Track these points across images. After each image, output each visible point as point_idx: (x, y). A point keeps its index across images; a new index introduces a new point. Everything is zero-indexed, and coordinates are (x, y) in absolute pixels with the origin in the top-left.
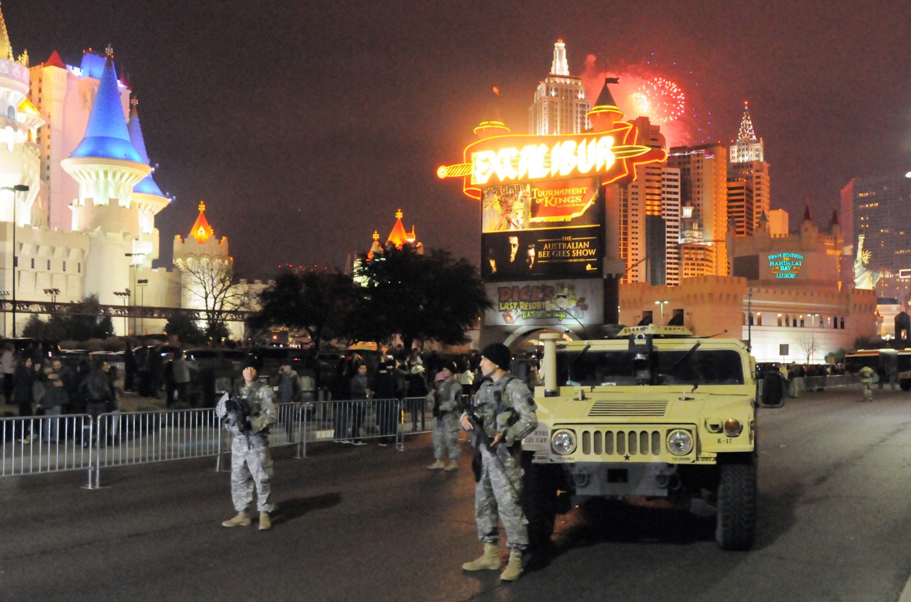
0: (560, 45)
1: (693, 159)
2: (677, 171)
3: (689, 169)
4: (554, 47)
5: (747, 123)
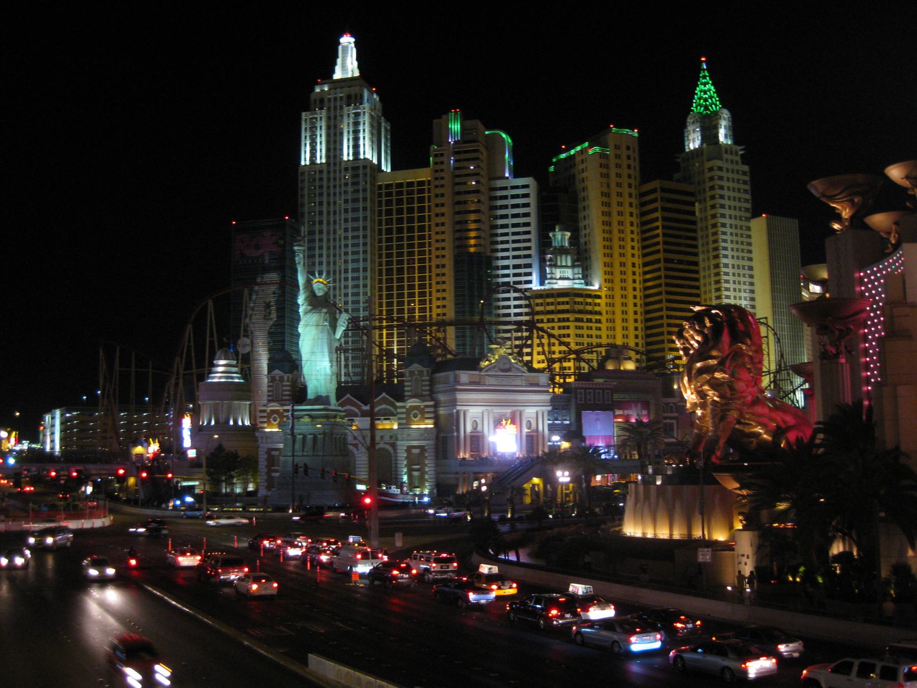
0: (347, 41)
1: (578, 159)
3: (574, 175)
4: (339, 43)
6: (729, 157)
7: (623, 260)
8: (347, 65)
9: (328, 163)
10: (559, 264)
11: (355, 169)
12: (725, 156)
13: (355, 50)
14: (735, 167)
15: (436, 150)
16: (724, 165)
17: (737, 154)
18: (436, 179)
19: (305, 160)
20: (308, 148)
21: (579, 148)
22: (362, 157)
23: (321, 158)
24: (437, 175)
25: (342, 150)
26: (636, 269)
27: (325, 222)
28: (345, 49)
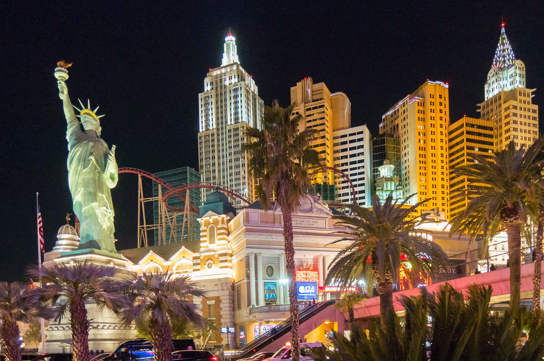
0: (230, 40)
1: (401, 111)
3: (398, 124)
4: (225, 42)
5: (504, 47)
6: (523, 98)
7: (435, 183)
9: (218, 129)
10: (385, 189)
11: (236, 129)
12: (519, 97)
13: (236, 47)
14: (527, 106)
16: (519, 105)
17: (528, 96)
19: (202, 128)
20: (204, 119)
21: (400, 103)
22: (240, 121)
26: (445, 190)
27: (217, 171)
28: (228, 46)
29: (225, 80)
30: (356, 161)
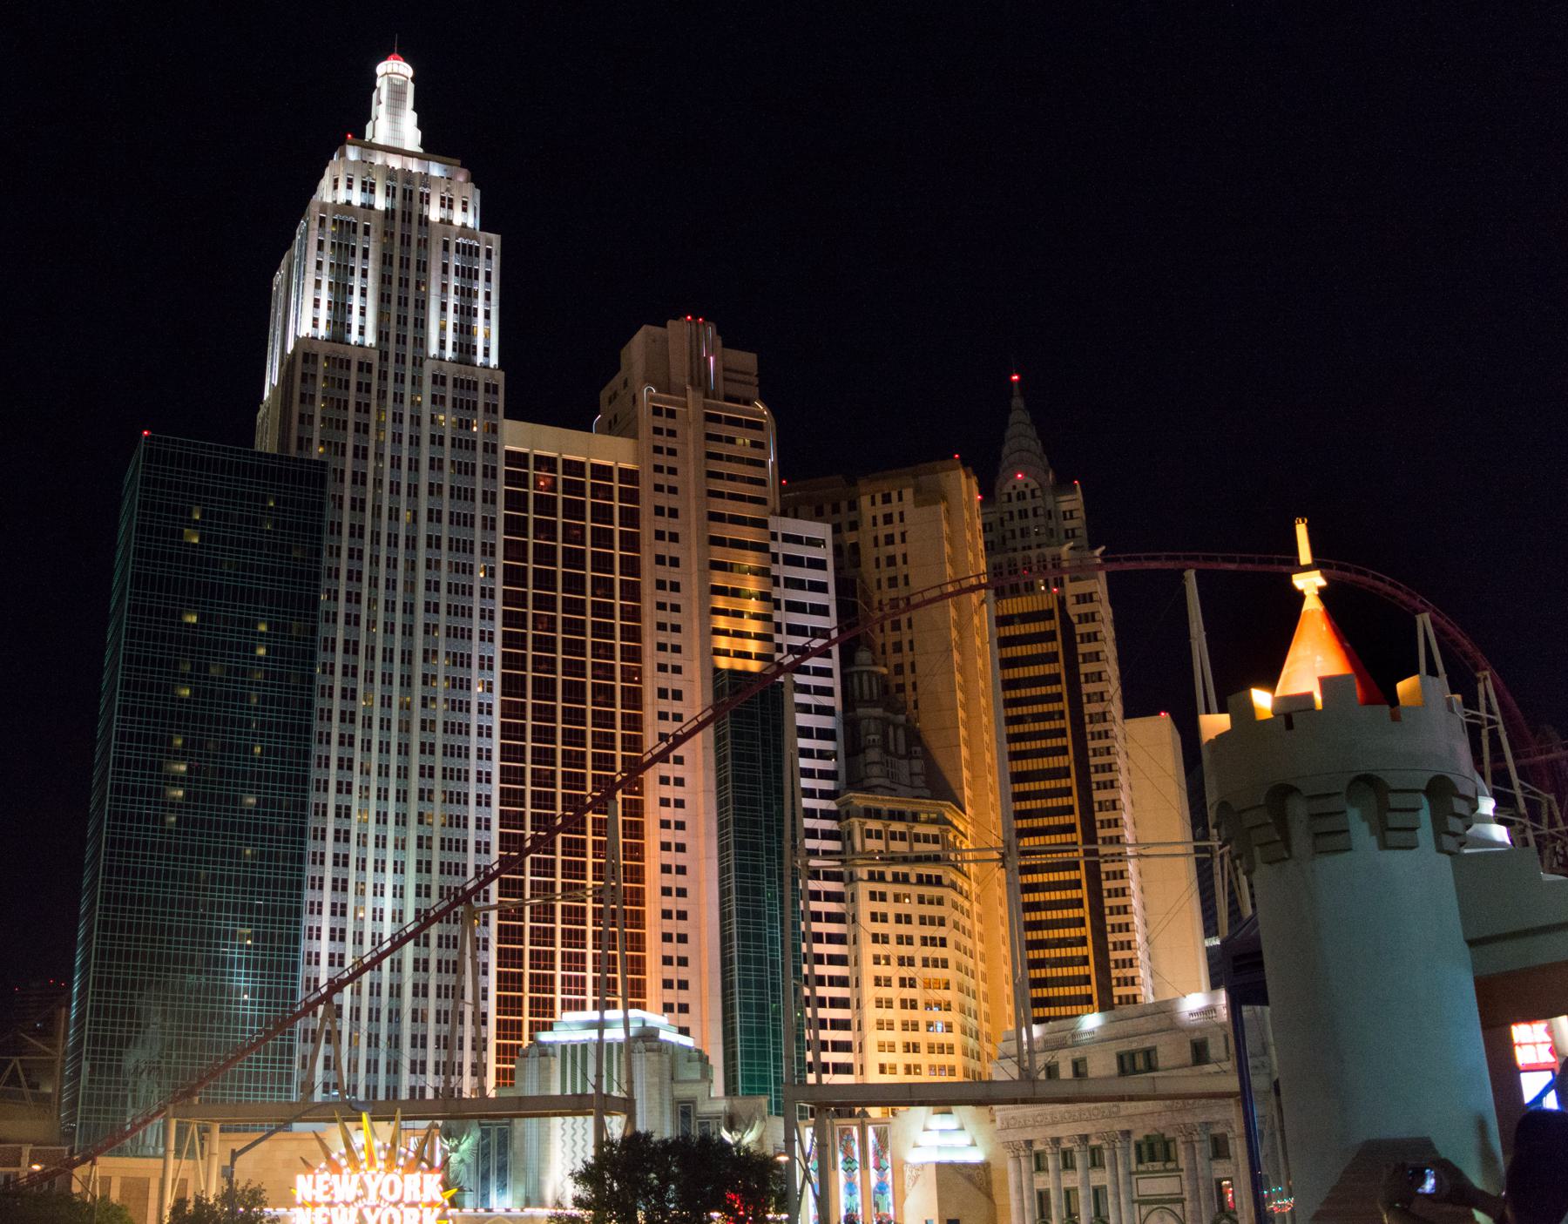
0: (394, 71)
2: (822, 530)
8: (395, 124)
9: (384, 356)
15: (652, 399)
18: (658, 469)
23: (364, 329)
24: (664, 460)
25: (421, 324)
29: (425, 199)
30: (805, 628)
